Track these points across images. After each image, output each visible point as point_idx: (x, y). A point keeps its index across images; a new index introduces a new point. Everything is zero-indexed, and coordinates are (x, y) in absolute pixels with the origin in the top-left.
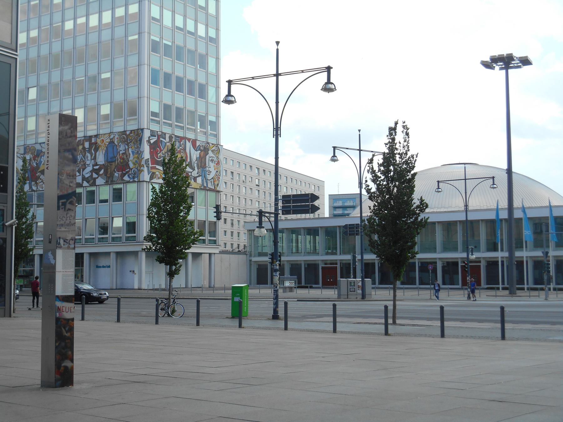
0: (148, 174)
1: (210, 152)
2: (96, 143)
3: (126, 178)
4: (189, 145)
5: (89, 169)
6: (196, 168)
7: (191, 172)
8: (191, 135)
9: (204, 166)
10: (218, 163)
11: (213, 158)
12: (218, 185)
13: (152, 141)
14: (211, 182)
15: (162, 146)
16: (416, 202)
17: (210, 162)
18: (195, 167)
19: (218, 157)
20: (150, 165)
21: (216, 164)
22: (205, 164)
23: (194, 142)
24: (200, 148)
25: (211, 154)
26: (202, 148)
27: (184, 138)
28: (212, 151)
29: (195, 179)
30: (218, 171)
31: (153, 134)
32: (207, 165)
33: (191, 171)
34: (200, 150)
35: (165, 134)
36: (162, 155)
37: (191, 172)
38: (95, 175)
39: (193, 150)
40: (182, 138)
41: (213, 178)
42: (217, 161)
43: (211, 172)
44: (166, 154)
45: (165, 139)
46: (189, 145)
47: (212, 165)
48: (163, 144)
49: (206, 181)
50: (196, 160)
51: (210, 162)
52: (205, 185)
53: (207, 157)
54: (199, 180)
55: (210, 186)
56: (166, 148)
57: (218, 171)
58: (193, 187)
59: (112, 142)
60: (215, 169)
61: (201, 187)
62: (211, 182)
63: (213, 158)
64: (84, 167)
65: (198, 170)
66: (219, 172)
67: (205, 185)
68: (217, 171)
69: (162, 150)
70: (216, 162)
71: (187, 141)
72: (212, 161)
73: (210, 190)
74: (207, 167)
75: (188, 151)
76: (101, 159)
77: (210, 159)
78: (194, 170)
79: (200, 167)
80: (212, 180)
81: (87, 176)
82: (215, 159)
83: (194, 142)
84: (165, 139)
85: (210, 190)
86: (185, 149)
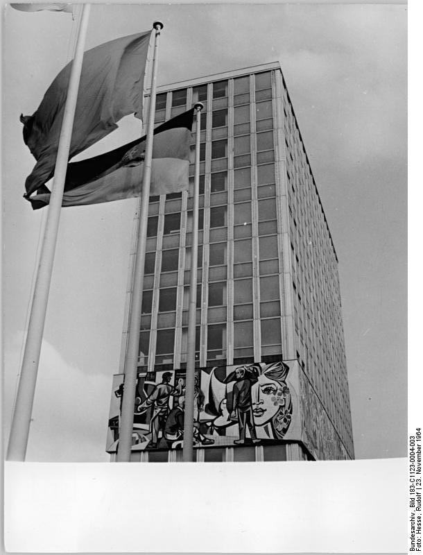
0: (115, 441)
6: (226, 413)
9: (246, 403)
10: (284, 392)
11: (270, 386)
12: (285, 431)
14: (266, 429)
15: (146, 392)
16: (412, 432)
17: (261, 393)
18: (221, 410)
19: (284, 382)
21: (279, 394)
22: (250, 399)
24: (235, 376)
25: (263, 379)
26: (239, 376)
29: (222, 431)
30: (284, 406)
32: (254, 400)
33: (213, 417)
34: (235, 378)
36: (146, 406)
37: (212, 421)
39: (215, 382)
41: (270, 420)
42: (280, 389)
43: (266, 410)
44: (155, 403)
45: (154, 380)
48: (149, 392)
49: (250, 430)
50: (226, 398)
51: (261, 393)
52: (248, 436)
53: (254, 388)
54: (233, 431)
55: (261, 434)
56: (156, 393)
57: (284, 406)
58: (217, 445)
60: (275, 404)
61: (239, 442)
62: (266, 429)
63: (270, 386)
65: (230, 411)
66: (287, 406)
67: (248, 436)
68: (281, 407)
69: (147, 399)
70: (279, 391)
71: (202, 372)
72: (267, 391)
74: (254, 404)
75: (204, 388)
77: (263, 388)
79: (236, 408)
80: (269, 424)
84: (154, 380)
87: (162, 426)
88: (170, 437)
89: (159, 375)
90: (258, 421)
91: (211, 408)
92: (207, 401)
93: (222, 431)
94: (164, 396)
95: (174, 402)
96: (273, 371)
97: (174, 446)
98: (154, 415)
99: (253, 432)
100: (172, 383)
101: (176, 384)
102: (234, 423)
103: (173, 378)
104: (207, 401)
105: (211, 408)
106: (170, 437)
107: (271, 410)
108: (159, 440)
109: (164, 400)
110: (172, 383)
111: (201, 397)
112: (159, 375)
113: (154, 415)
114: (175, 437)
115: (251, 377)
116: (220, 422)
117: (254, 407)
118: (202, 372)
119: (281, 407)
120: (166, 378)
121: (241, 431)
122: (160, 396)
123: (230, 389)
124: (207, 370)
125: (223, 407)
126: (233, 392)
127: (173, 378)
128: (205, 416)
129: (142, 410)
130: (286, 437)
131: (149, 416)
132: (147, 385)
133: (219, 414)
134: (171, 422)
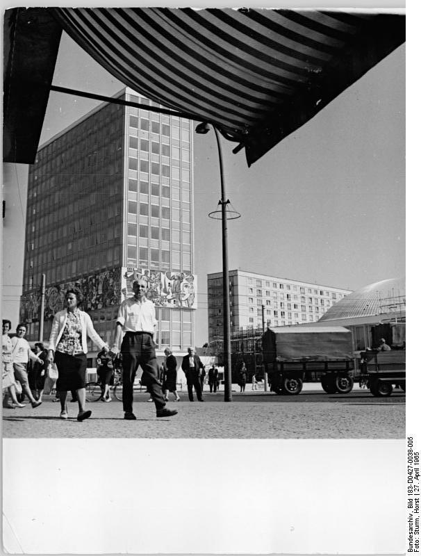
1: (184, 280)
2: (98, 279)
3: (112, 303)
4: (163, 276)
5: (95, 297)
6: (171, 294)
13: (128, 276)
20: (127, 293)
25: (185, 281)
28: (186, 279)
29: (169, 301)
33: (165, 294)
38: (97, 302)
47: (186, 289)
53: (182, 284)
55: (185, 305)
59: (106, 278)
64: (93, 296)
65: (173, 293)
72: (186, 286)
73: (185, 309)
76: (100, 292)
81: (93, 303)
82: (189, 285)
85: (185, 309)
86: (160, 279)
89: (143, 271)
90: (183, 299)
92: (163, 287)
93: (169, 301)
99: (181, 303)
100: (149, 275)
104: (163, 287)
107: (187, 296)
110: (149, 275)
111: (161, 285)
112: (143, 271)
115: (180, 279)
116: (169, 297)
120: (146, 273)
124: (164, 273)
125: (170, 291)
128: (163, 294)
130: (193, 307)
132: (137, 275)
133: (168, 293)
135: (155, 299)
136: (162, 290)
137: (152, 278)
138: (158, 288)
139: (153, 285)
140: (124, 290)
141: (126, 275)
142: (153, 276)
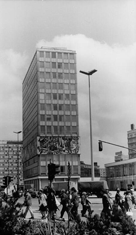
4: (61, 139)
6: (65, 147)
7: (62, 149)
8: (60, 136)
12: (78, 152)
13: (41, 140)
18: (64, 147)
20: (40, 149)
23: (64, 138)
25: (73, 140)
26: (67, 139)
27: (59, 137)
29: (64, 151)
31: (41, 137)
34: (67, 140)
35: (48, 137)
39: (63, 141)
40: (57, 137)
41: (75, 150)
45: (48, 138)
46: (61, 139)
52: (70, 152)
65: (66, 147)
71: (59, 138)
72: (74, 143)
75: (60, 140)
78: (64, 147)
82: (76, 142)
83: (64, 138)
87: (50, 149)
88: (52, 152)
91: (61, 146)
92: (60, 144)
93: (64, 151)
94: (50, 142)
95: (53, 144)
96: (75, 139)
97: (54, 153)
98: (48, 146)
101: (53, 140)
102: (67, 149)
103: (52, 138)
104: (60, 144)
105: (61, 146)
106: (52, 152)
107: (75, 147)
108: (50, 152)
109: (50, 143)
110: (52, 139)
113: (48, 146)
114: (53, 152)
116: (64, 149)
117: (71, 146)
118: (59, 138)
119: (77, 147)
121: (69, 151)
122: (49, 143)
123: (66, 142)
126: (66, 143)
127: (52, 138)
128: (60, 147)
129: (45, 145)
131: (47, 147)
132: (46, 140)
133: (64, 147)
134: (52, 148)
135: (56, 151)
136: (60, 146)
137: (54, 140)
138: (57, 145)
139: (54, 143)
140: (38, 148)
141: (39, 140)
142: (54, 139)
